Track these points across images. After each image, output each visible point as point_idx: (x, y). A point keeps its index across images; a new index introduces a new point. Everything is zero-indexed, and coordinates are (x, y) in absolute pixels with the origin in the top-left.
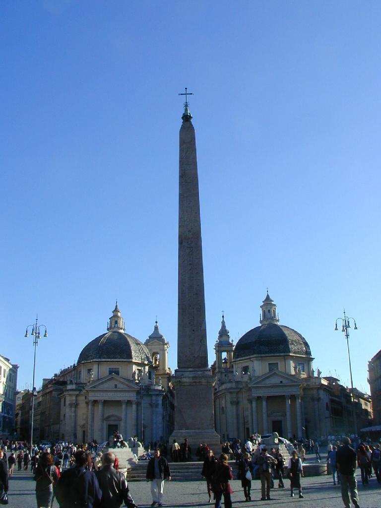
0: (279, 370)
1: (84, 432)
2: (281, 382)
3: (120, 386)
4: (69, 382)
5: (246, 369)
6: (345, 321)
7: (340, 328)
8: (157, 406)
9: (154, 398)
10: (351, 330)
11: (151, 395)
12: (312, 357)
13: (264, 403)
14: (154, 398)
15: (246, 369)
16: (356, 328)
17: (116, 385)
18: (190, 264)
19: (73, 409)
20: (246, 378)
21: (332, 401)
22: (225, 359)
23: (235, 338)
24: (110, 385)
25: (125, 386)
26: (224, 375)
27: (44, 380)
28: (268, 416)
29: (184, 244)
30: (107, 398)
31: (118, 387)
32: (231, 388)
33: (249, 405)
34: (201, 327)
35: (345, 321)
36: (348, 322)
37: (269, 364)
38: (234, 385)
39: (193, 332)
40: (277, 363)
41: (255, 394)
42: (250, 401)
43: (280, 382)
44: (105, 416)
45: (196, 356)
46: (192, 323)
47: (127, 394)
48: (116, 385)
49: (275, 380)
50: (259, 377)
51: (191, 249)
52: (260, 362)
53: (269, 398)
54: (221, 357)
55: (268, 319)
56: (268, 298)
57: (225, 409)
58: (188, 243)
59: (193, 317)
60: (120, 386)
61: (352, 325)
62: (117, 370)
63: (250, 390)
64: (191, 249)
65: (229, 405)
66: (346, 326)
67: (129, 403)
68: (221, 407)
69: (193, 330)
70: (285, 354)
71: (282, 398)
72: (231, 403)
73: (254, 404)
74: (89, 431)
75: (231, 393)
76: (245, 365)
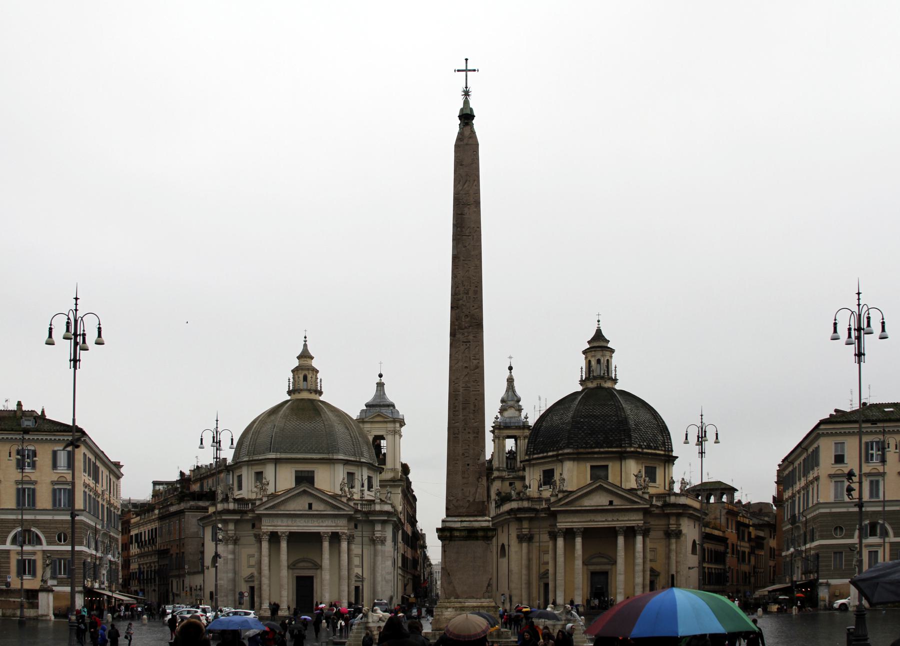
0: (610, 480)
1: (252, 589)
2: (611, 503)
3: (318, 507)
4: (220, 497)
5: (548, 478)
6: (702, 429)
7: (693, 439)
8: (383, 541)
9: (378, 527)
10: (709, 445)
11: (373, 523)
12: (674, 454)
13: (579, 541)
14: (378, 527)
15: (548, 478)
16: (717, 442)
17: (310, 506)
18: (466, 367)
19: (231, 547)
20: (547, 493)
21: (706, 537)
22: (510, 452)
23: (532, 413)
24: (299, 505)
25: (329, 508)
26: (507, 483)
27: (155, 483)
28: (585, 563)
29: (457, 336)
30: (294, 529)
31: (314, 507)
32: (519, 510)
33: (551, 544)
34: (479, 459)
35: (702, 429)
36: (705, 432)
37: (592, 467)
38: (526, 504)
39: (468, 467)
40: (607, 467)
41: (563, 523)
42: (553, 536)
43: (608, 503)
44: (291, 562)
45: (471, 500)
46: (466, 455)
47: (329, 522)
48: (310, 506)
49: (600, 500)
50: (571, 492)
51: (468, 345)
52: (576, 463)
53: (589, 534)
54: (504, 446)
55: (595, 378)
56: (599, 336)
57: (506, 547)
58: (463, 334)
59: (469, 446)
60: (318, 507)
61: (711, 436)
62: (310, 475)
63: (553, 515)
64: (468, 344)
65: (514, 541)
66: (701, 439)
67: (335, 538)
68: (500, 544)
69: (468, 465)
70: (623, 449)
71: (612, 533)
72: (518, 537)
73: (560, 542)
74: (265, 588)
75: (520, 520)
76: (548, 467)
